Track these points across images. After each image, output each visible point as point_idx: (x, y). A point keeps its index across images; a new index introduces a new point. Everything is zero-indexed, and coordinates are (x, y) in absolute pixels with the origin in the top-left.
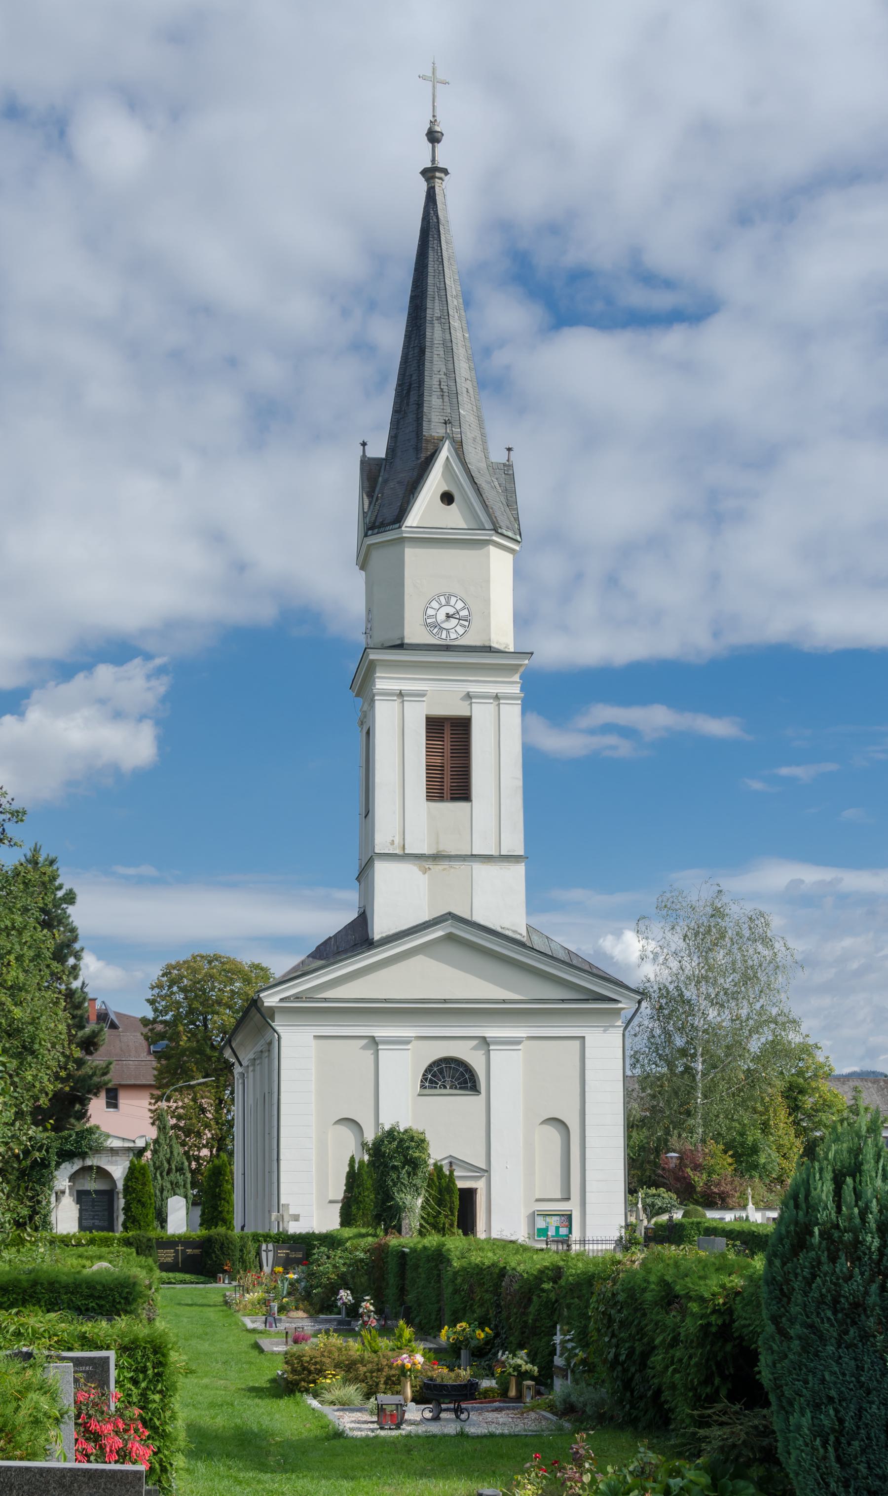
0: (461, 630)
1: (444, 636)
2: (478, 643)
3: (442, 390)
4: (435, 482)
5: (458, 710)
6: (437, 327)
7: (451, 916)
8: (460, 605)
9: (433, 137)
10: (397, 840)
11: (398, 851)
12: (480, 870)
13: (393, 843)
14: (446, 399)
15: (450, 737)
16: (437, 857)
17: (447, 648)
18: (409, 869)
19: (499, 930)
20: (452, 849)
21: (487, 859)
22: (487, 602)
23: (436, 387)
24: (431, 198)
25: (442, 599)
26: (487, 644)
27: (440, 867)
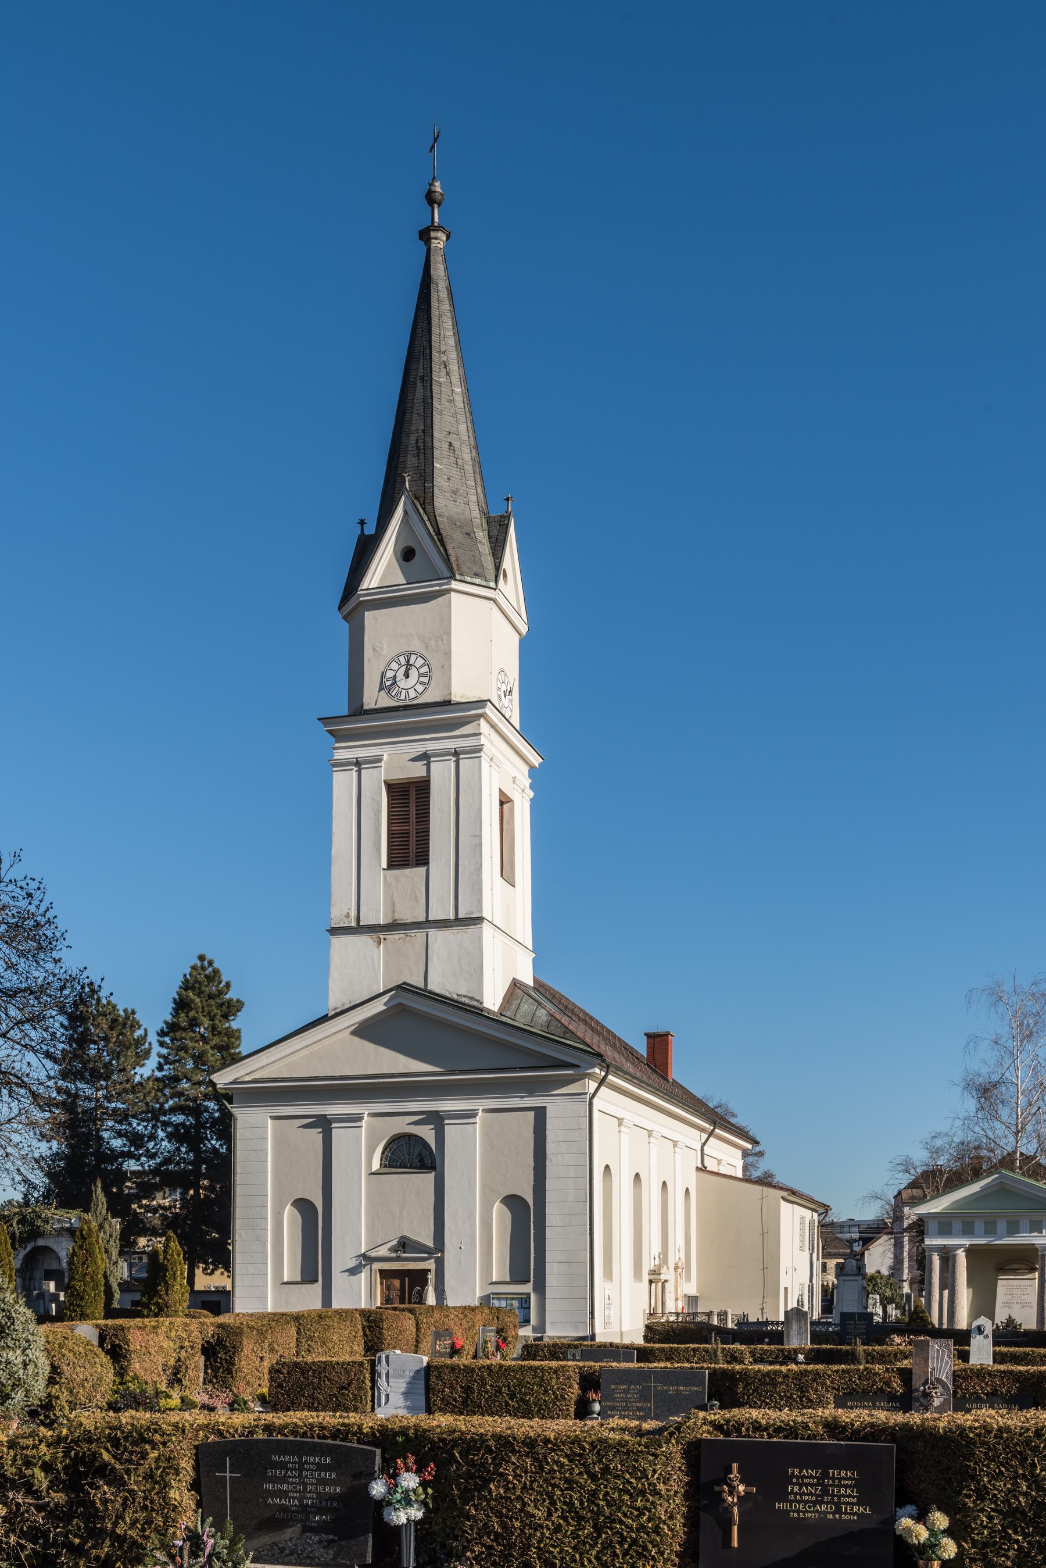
0: (420, 688)
1: (403, 697)
2: (438, 699)
3: (418, 448)
5: (418, 771)
6: (419, 384)
7: (403, 988)
8: (420, 662)
10: (353, 913)
11: (353, 924)
12: (437, 936)
13: (348, 916)
14: (422, 456)
16: (393, 926)
17: (406, 707)
18: (363, 942)
19: (455, 997)
21: (443, 924)
22: (448, 654)
23: (412, 448)
25: (402, 659)
26: (447, 699)
27: (396, 937)
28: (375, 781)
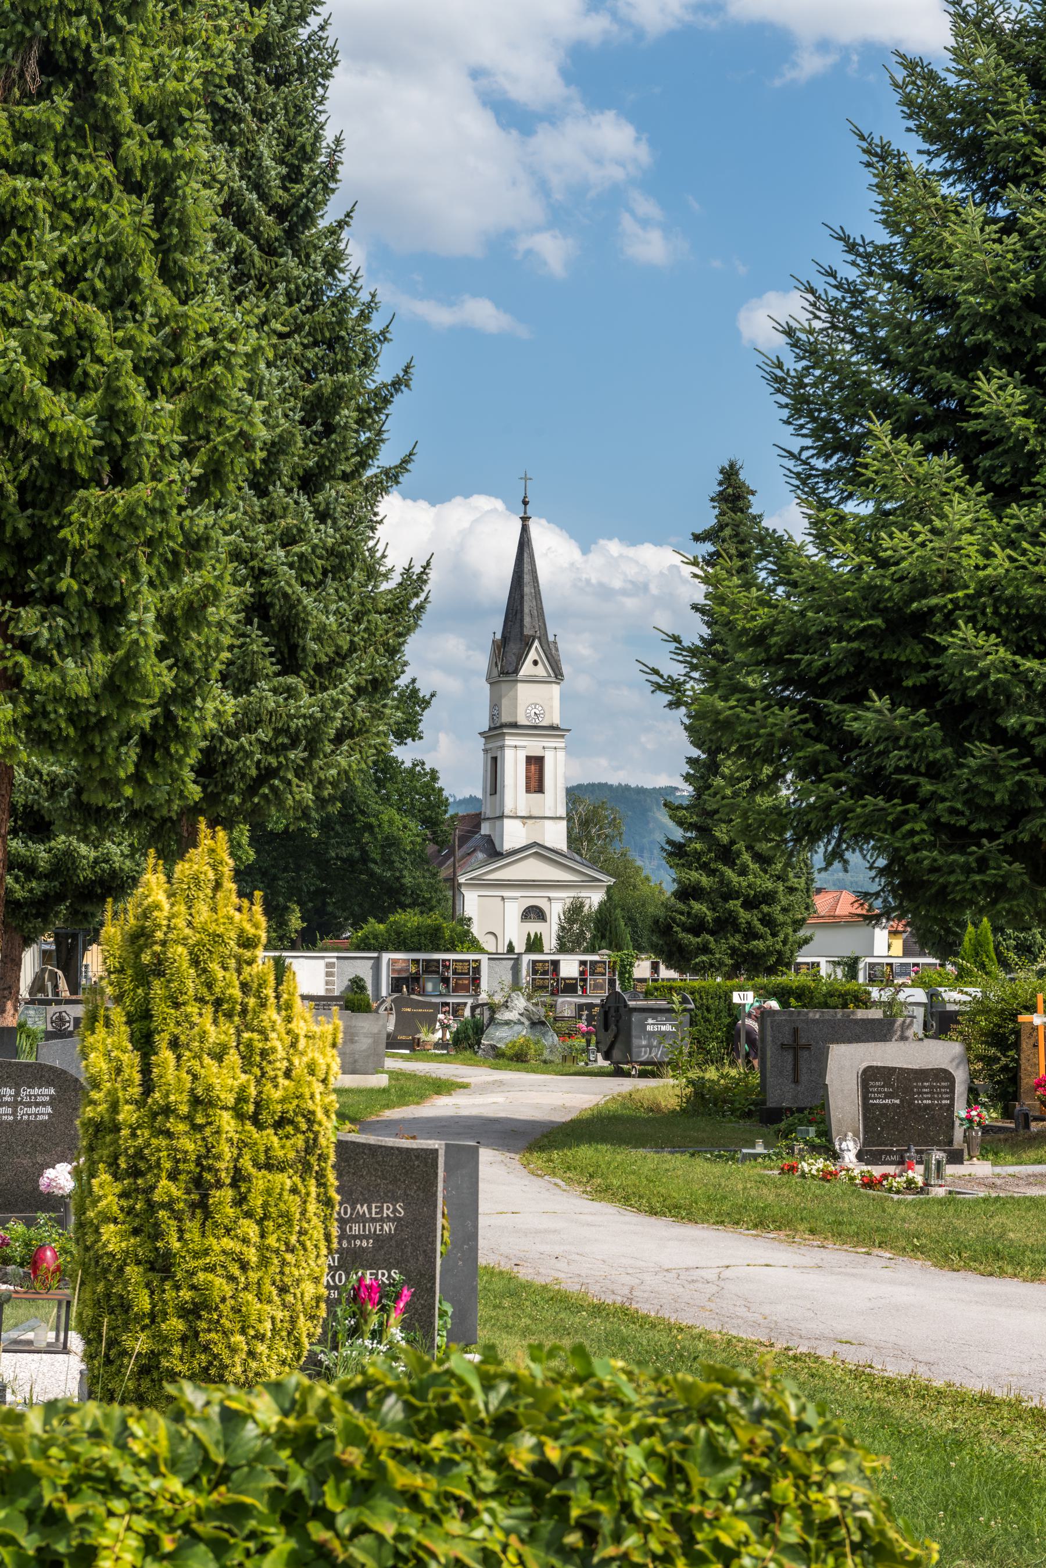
4: (532, 655)
7: (536, 844)
9: (525, 503)
12: (547, 822)
15: (536, 763)
18: (517, 823)
20: (535, 814)
24: (525, 530)
28: (522, 756)
